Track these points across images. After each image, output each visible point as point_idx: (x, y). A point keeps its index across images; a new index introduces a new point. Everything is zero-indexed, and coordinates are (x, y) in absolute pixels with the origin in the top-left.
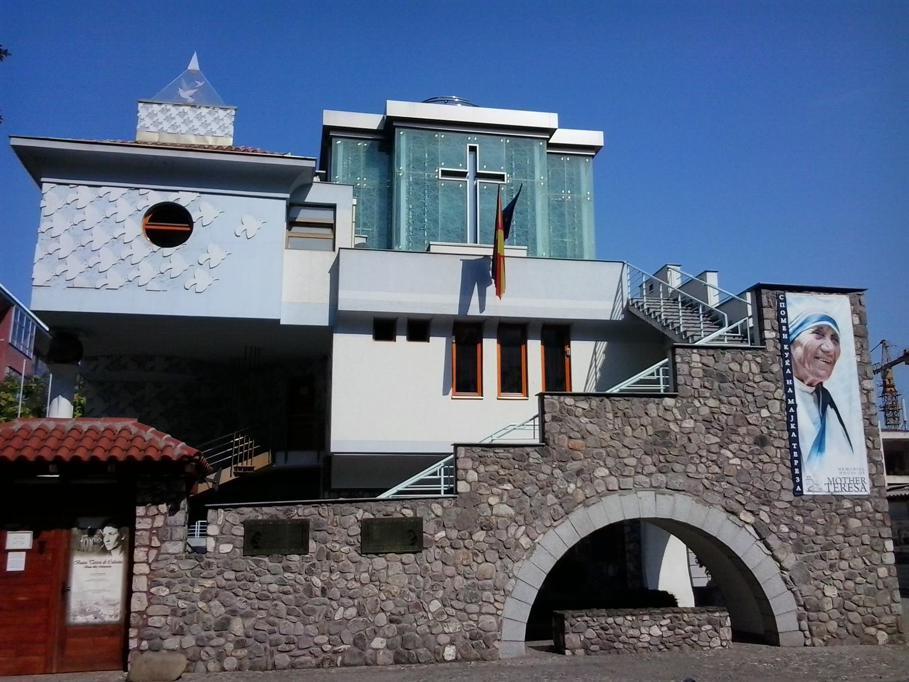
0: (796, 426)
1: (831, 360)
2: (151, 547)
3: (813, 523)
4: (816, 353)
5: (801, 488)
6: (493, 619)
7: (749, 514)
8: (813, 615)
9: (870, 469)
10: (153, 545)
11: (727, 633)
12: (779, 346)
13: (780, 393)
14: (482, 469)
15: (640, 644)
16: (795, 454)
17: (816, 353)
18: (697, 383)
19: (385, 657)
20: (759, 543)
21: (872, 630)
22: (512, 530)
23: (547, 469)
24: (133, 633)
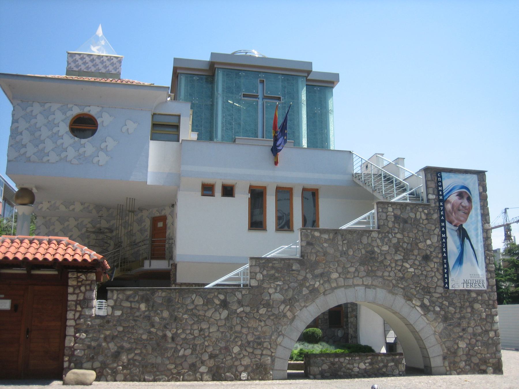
0: (446, 249)
2: (76, 311)
4: (459, 207)
5: (448, 285)
7: (418, 300)
9: (487, 275)
10: (77, 309)
12: (437, 204)
13: (437, 231)
15: (353, 373)
16: (445, 266)
17: (459, 207)
18: (391, 225)
20: (423, 317)
22: (282, 307)
23: (303, 273)
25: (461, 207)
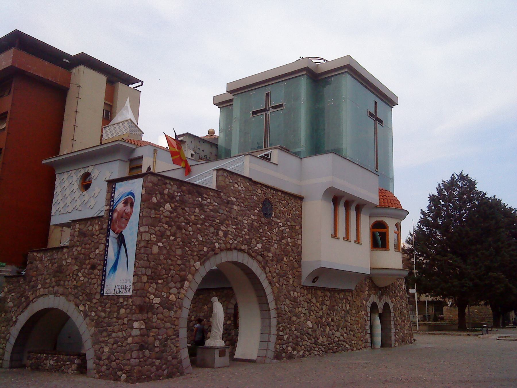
3: (105, 311)
11: (74, 367)
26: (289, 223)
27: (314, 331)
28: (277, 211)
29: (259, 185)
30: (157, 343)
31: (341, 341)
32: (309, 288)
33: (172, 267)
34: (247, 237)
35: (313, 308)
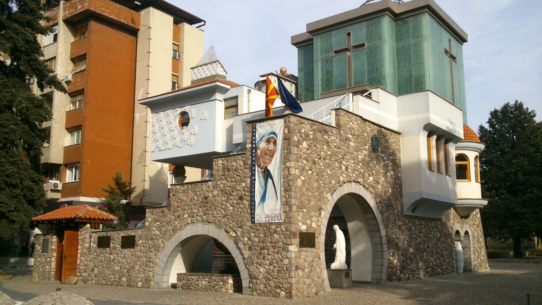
1: (272, 154)
6: (152, 274)
8: (255, 281)
14: (152, 217)
17: (266, 152)
19: (125, 284)
21: (278, 291)
23: (169, 216)
24: (77, 270)
25: (268, 151)
26: (391, 157)
27: (415, 256)
28: (382, 146)
29: (368, 123)
30: (306, 264)
31: (434, 266)
32: (409, 217)
33: (312, 198)
34: (362, 171)
35: (413, 236)
